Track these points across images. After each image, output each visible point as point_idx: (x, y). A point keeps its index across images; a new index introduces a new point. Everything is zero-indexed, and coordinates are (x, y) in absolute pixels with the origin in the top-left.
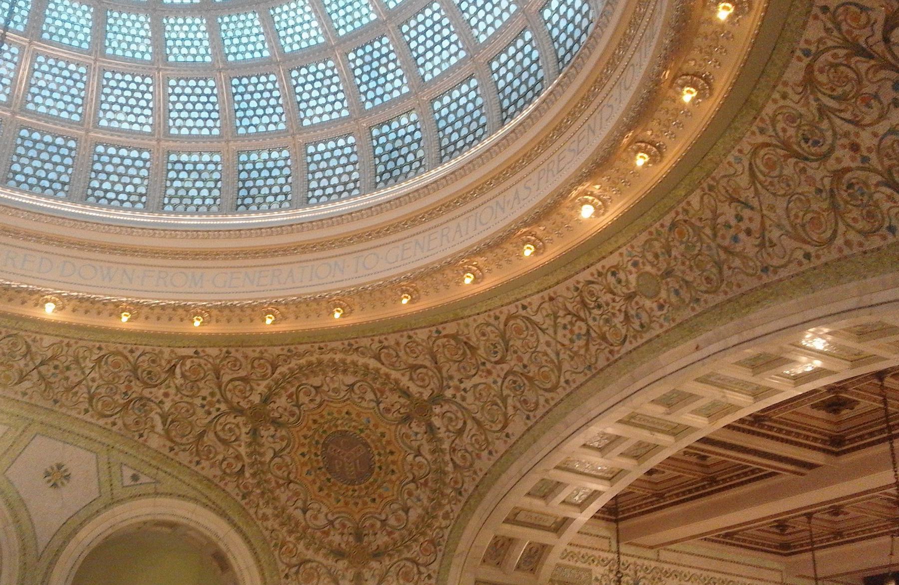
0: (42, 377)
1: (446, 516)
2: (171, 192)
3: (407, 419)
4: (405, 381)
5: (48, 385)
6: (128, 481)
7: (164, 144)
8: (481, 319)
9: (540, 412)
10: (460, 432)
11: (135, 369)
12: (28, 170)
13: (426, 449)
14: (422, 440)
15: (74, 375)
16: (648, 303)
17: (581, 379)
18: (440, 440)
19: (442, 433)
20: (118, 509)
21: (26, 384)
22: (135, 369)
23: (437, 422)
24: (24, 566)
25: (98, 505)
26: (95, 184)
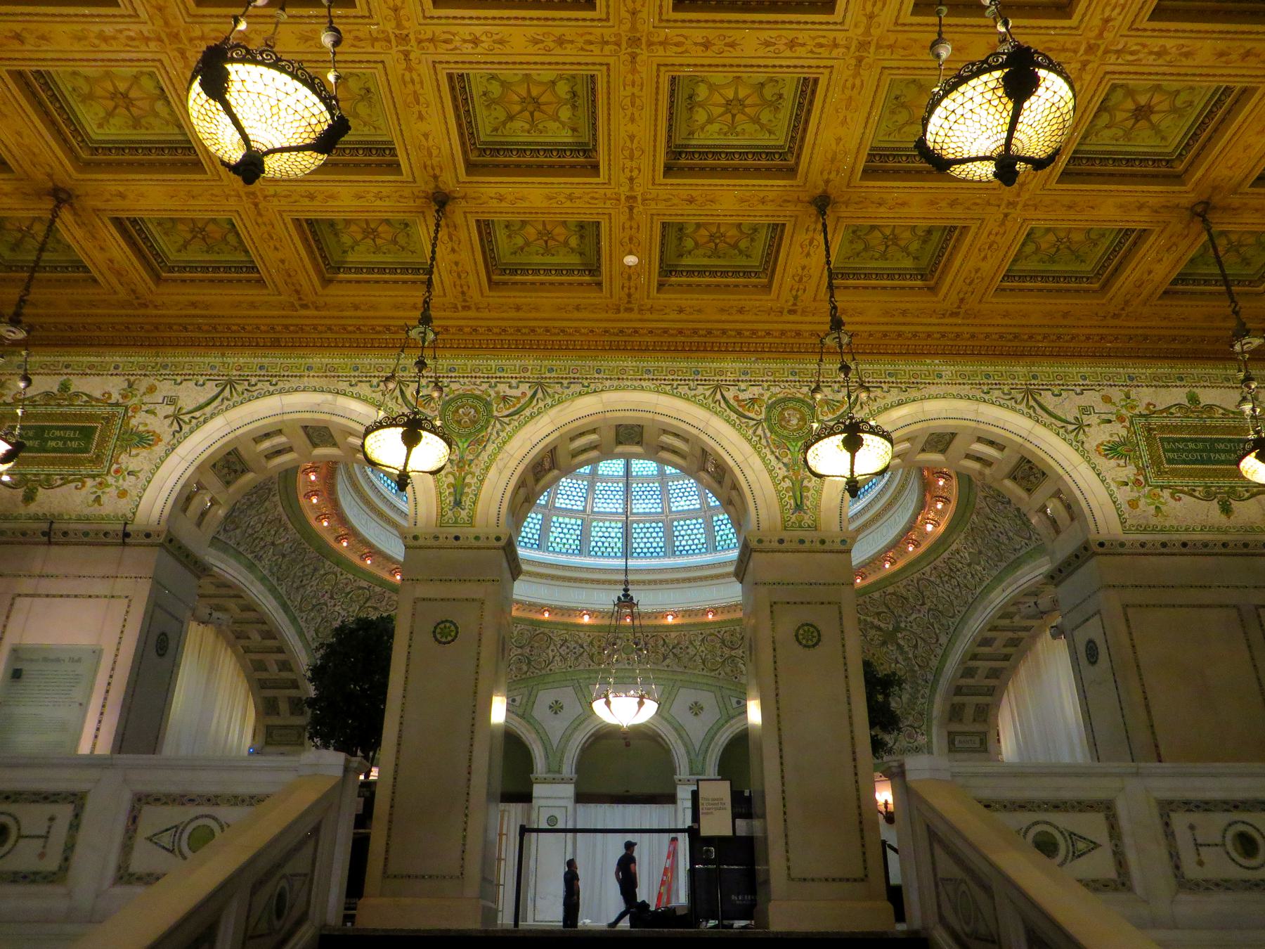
0: (675, 655)
1: (923, 697)
2: (718, 538)
3: (884, 643)
4: (876, 622)
5: (679, 659)
6: (735, 705)
7: (709, 513)
8: (904, 582)
9: (952, 629)
10: (916, 646)
11: (723, 642)
12: (642, 545)
13: (900, 659)
14: (897, 654)
15: (691, 651)
16: (978, 568)
17: (964, 609)
18: (907, 653)
19: (906, 649)
20: (733, 722)
21: (668, 661)
22: (723, 642)
23: (902, 643)
24: (691, 762)
25: (722, 721)
26: (677, 543)
